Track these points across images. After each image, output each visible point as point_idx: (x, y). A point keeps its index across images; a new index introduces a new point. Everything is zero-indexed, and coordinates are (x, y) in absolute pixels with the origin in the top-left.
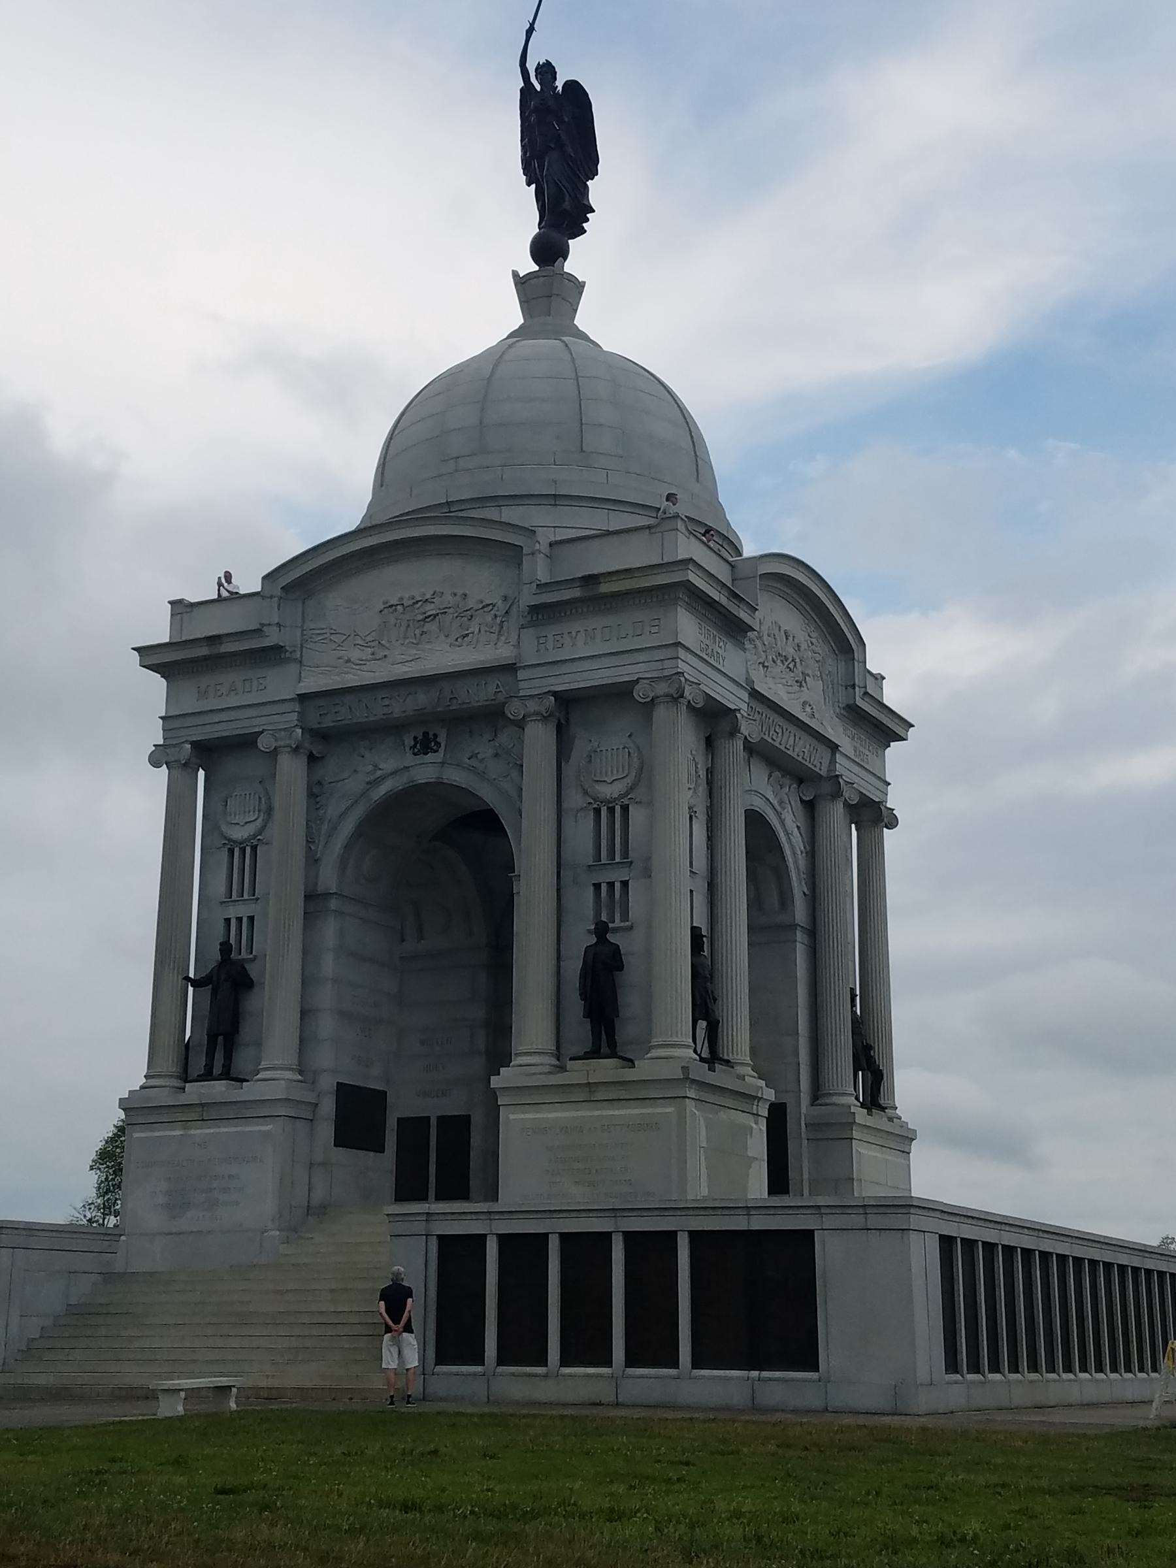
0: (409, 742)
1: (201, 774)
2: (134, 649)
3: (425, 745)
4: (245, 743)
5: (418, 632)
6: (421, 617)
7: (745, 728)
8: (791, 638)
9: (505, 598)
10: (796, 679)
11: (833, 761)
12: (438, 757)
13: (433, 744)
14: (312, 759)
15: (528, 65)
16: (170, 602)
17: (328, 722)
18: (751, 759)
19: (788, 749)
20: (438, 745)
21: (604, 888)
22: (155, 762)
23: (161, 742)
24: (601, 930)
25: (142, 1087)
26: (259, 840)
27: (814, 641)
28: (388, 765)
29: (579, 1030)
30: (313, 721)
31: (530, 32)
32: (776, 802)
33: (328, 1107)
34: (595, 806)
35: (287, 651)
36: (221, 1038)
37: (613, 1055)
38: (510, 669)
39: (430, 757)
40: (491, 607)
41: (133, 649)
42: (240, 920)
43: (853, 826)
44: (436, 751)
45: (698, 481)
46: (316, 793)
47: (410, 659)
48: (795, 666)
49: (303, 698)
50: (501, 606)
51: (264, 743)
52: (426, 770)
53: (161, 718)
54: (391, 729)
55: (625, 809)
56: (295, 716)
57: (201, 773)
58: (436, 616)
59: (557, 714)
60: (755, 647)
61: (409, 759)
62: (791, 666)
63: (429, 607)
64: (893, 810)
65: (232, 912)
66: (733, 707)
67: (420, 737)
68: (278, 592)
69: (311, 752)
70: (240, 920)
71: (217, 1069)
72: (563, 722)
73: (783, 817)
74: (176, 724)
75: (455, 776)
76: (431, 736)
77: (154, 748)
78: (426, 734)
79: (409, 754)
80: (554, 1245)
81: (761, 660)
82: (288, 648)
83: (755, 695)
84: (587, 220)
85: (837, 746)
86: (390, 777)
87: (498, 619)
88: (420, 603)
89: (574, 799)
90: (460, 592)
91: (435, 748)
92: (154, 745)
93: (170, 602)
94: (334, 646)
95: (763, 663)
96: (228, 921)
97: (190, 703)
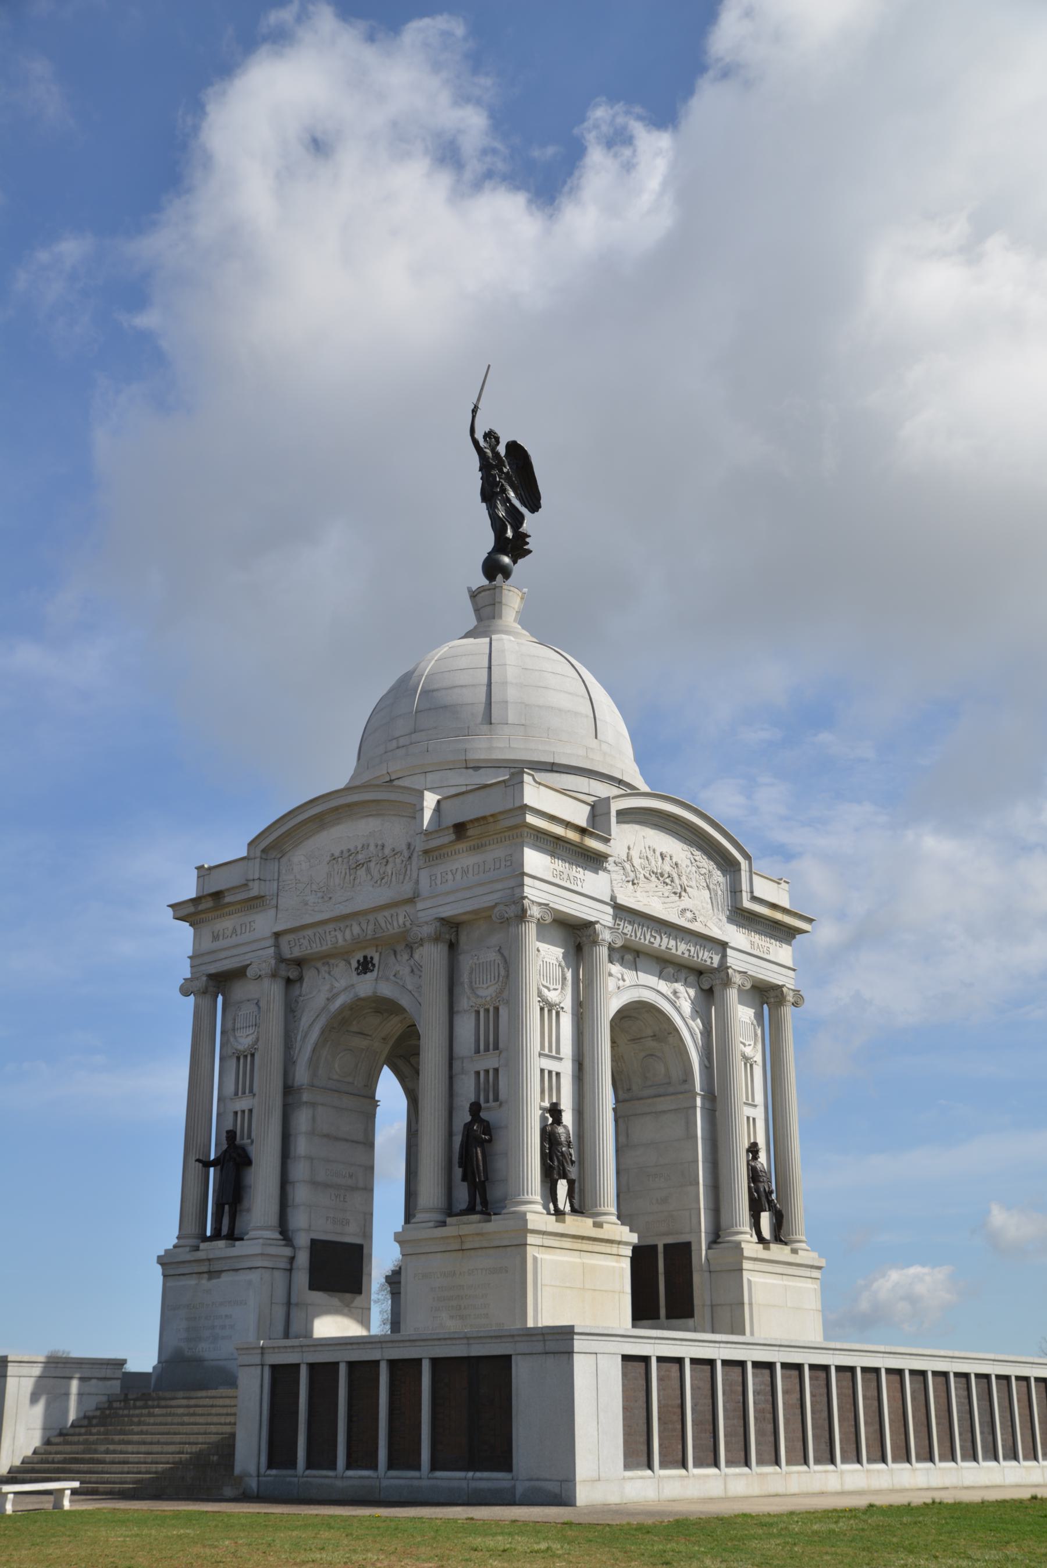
1: (220, 998)
2: (169, 906)
3: (365, 966)
4: (239, 973)
5: (352, 877)
6: (354, 866)
7: (606, 936)
8: (667, 859)
9: (409, 845)
10: (674, 890)
11: (724, 956)
13: (370, 965)
14: (289, 982)
15: (476, 436)
16: (196, 868)
18: (637, 959)
19: (671, 949)
20: (374, 965)
22: (185, 991)
23: (189, 976)
24: (475, 1108)
25: (175, 1247)
27: (697, 858)
28: (342, 983)
29: (462, 1193)
30: (287, 954)
31: (474, 411)
32: (669, 993)
33: (303, 1259)
34: (476, 1008)
36: (227, 1207)
37: (481, 1213)
39: (369, 975)
40: (399, 854)
41: (169, 906)
43: (765, 1006)
44: (372, 971)
45: (596, 738)
46: (291, 1010)
48: (672, 881)
49: (277, 935)
50: (406, 854)
51: (250, 972)
52: (366, 986)
53: (189, 957)
55: (497, 1009)
56: (272, 950)
57: (220, 998)
58: (363, 864)
59: (447, 936)
60: (624, 869)
61: (355, 978)
62: (668, 881)
64: (799, 991)
67: (362, 960)
68: (258, 854)
69: (289, 978)
70: (243, 1112)
71: (225, 1230)
73: (678, 1004)
75: (386, 990)
76: (369, 959)
78: (365, 957)
79: (355, 973)
80: (343, 1370)
81: (630, 879)
84: (527, 543)
85: (727, 943)
86: (343, 993)
87: (404, 862)
88: (353, 855)
89: (464, 1003)
90: (380, 843)
91: (371, 968)
92: (184, 979)
93: (196, 868)
95: (633, 881)
97: (207, 945)
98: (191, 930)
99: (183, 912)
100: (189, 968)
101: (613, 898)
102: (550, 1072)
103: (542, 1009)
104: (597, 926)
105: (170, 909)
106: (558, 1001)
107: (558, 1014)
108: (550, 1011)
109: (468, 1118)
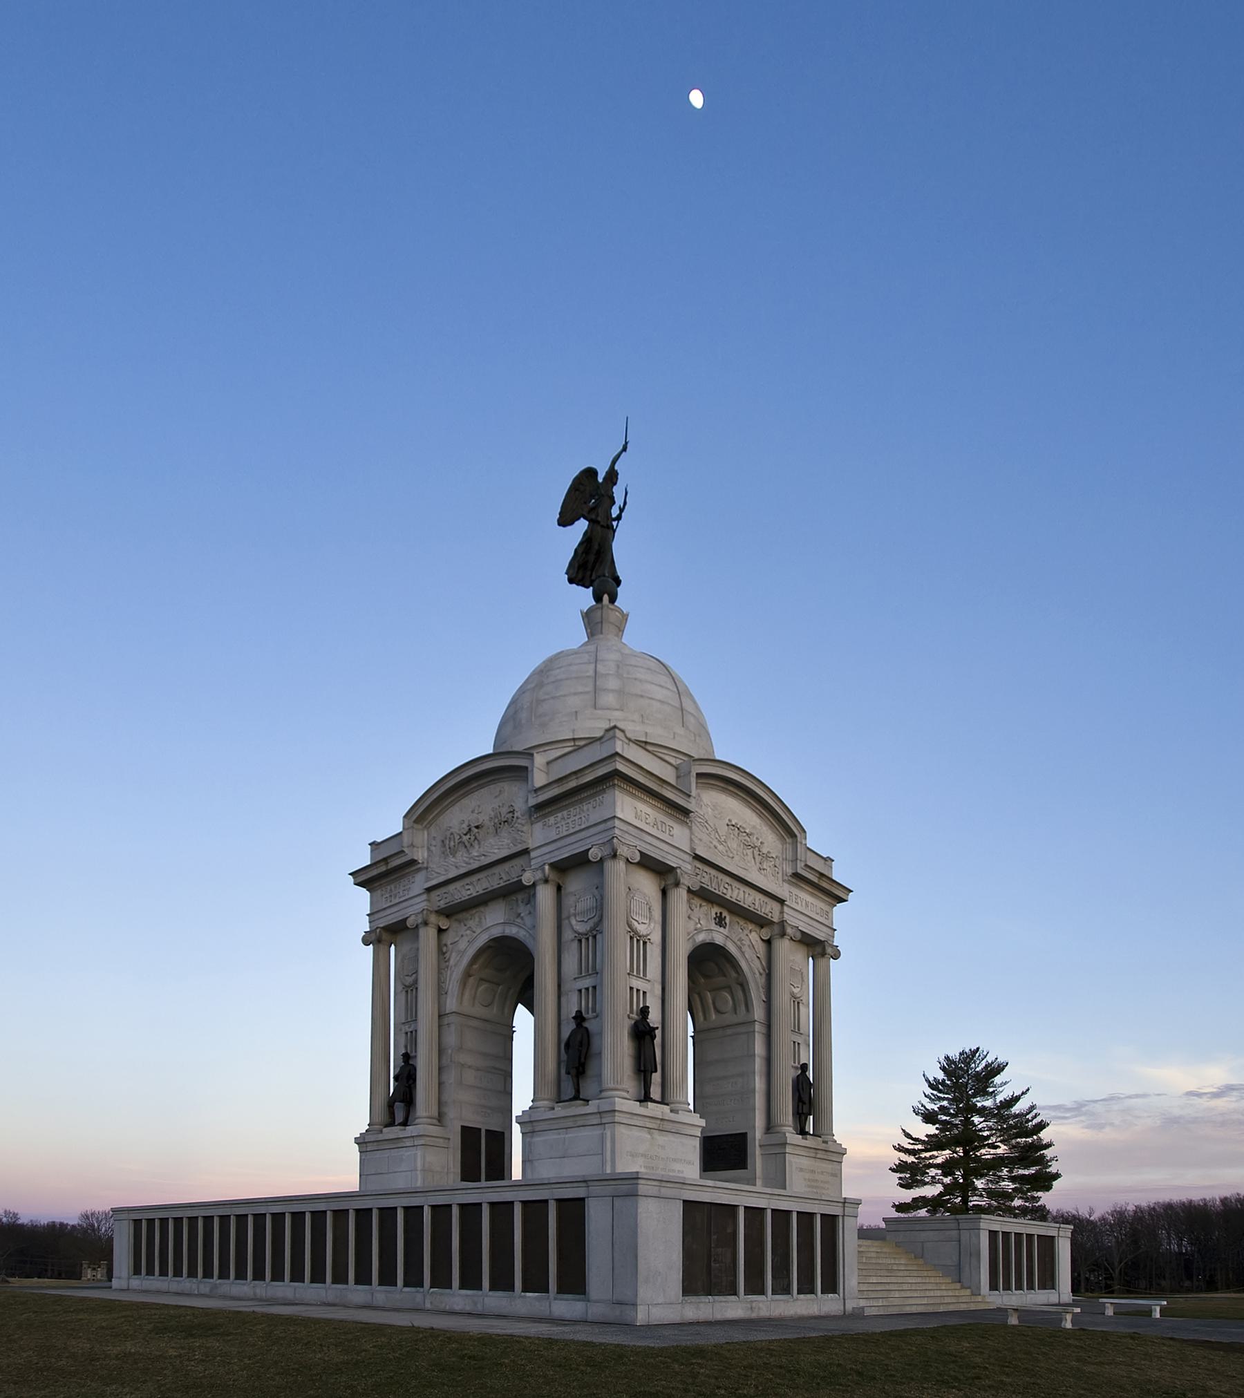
2: (350, 874)
7: (686, 881)
16: (370, 844)
17: (442, 904)
22: (366, 942)
23: (368, 930)
35: (419, 863)
41: (350, 874)
46: (441, 952)
53: (368, 915)
55: (595, 937)
57: (393, 946)
66: (674, 865)
72: (561, 884)
74: (372, 916)
77: (364, 934)
82: (420, 861)
83: (697, 857)
89: (568, 935)
93: (370, 844)
98: (368, 893)
99: (362, 878)
100: (368, 924)
101: (693, 849)
102: (638, 991)
103: (631, 938)
104: (678, 871)
105: (351, 877)
106: (645, 933)
107: (645, 943)
108: (638, 941)
109: (573, 1026)
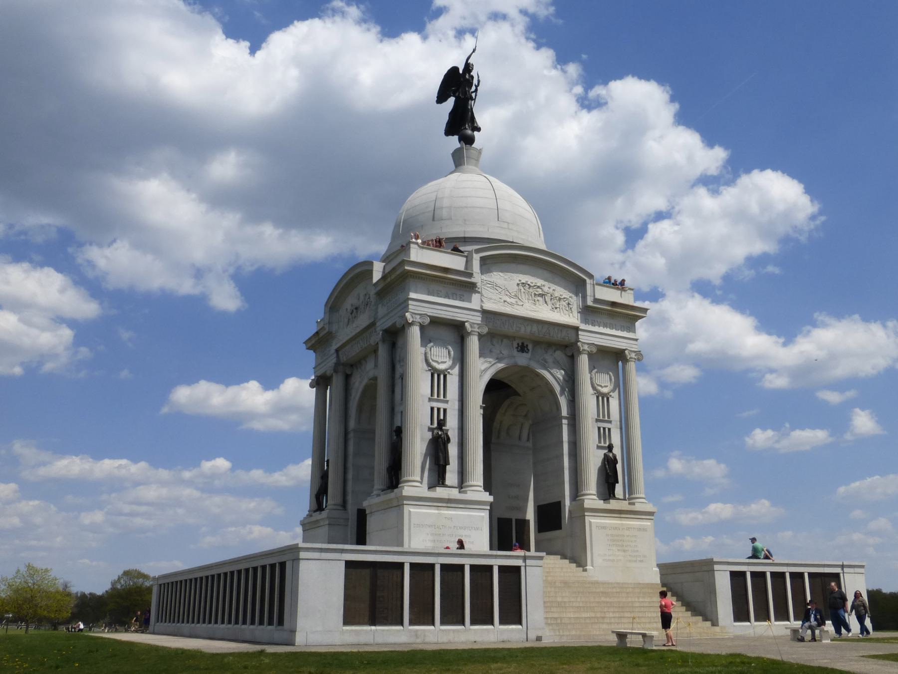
0: (515, 345)
3: (523, 348)
12: (529, 355)
13: (526, 349)
20: (528, 350)
21: (602, 429)
26: (449, 372)
38: (577, 329)
39: (524, 354)
40: (566, 299)
42: (439, 409)
44: (527, 352)
47: (533, 310)
54: (511, 338)
61: (515, 352)
63: (538, 290)
65: (436, 405)
67: (520, 344)
76: (525, 344)
78: (523, 344)
79: (515, 350)
94: (497, 292)
96: (432, 409)
